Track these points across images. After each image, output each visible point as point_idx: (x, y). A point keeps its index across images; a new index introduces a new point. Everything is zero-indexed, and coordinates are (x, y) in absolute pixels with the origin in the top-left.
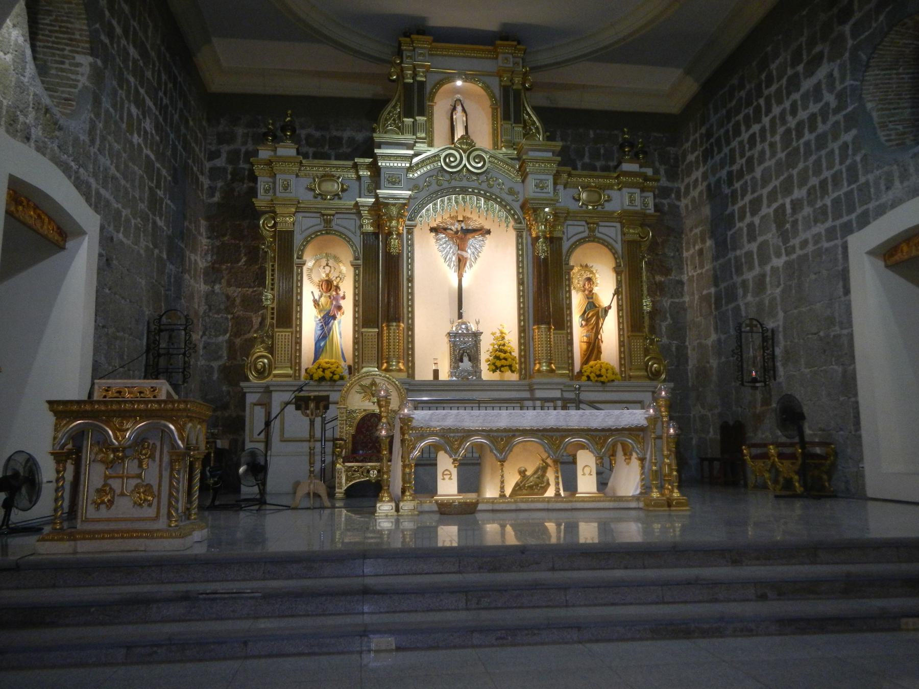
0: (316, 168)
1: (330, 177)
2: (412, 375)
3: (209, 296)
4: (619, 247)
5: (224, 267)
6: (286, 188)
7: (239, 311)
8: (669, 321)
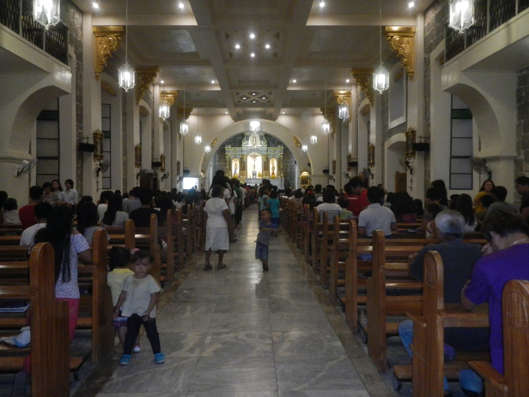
0: (234, 148)
1: (235, 150)
2: (247, 177)
3: (218, 164)
4: (277, 159)
5: (220, 160)
6: (230, 151)
7: (222, 167)
8: (289, 167)
